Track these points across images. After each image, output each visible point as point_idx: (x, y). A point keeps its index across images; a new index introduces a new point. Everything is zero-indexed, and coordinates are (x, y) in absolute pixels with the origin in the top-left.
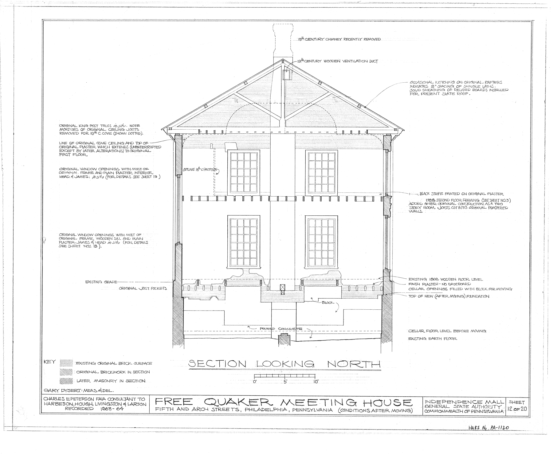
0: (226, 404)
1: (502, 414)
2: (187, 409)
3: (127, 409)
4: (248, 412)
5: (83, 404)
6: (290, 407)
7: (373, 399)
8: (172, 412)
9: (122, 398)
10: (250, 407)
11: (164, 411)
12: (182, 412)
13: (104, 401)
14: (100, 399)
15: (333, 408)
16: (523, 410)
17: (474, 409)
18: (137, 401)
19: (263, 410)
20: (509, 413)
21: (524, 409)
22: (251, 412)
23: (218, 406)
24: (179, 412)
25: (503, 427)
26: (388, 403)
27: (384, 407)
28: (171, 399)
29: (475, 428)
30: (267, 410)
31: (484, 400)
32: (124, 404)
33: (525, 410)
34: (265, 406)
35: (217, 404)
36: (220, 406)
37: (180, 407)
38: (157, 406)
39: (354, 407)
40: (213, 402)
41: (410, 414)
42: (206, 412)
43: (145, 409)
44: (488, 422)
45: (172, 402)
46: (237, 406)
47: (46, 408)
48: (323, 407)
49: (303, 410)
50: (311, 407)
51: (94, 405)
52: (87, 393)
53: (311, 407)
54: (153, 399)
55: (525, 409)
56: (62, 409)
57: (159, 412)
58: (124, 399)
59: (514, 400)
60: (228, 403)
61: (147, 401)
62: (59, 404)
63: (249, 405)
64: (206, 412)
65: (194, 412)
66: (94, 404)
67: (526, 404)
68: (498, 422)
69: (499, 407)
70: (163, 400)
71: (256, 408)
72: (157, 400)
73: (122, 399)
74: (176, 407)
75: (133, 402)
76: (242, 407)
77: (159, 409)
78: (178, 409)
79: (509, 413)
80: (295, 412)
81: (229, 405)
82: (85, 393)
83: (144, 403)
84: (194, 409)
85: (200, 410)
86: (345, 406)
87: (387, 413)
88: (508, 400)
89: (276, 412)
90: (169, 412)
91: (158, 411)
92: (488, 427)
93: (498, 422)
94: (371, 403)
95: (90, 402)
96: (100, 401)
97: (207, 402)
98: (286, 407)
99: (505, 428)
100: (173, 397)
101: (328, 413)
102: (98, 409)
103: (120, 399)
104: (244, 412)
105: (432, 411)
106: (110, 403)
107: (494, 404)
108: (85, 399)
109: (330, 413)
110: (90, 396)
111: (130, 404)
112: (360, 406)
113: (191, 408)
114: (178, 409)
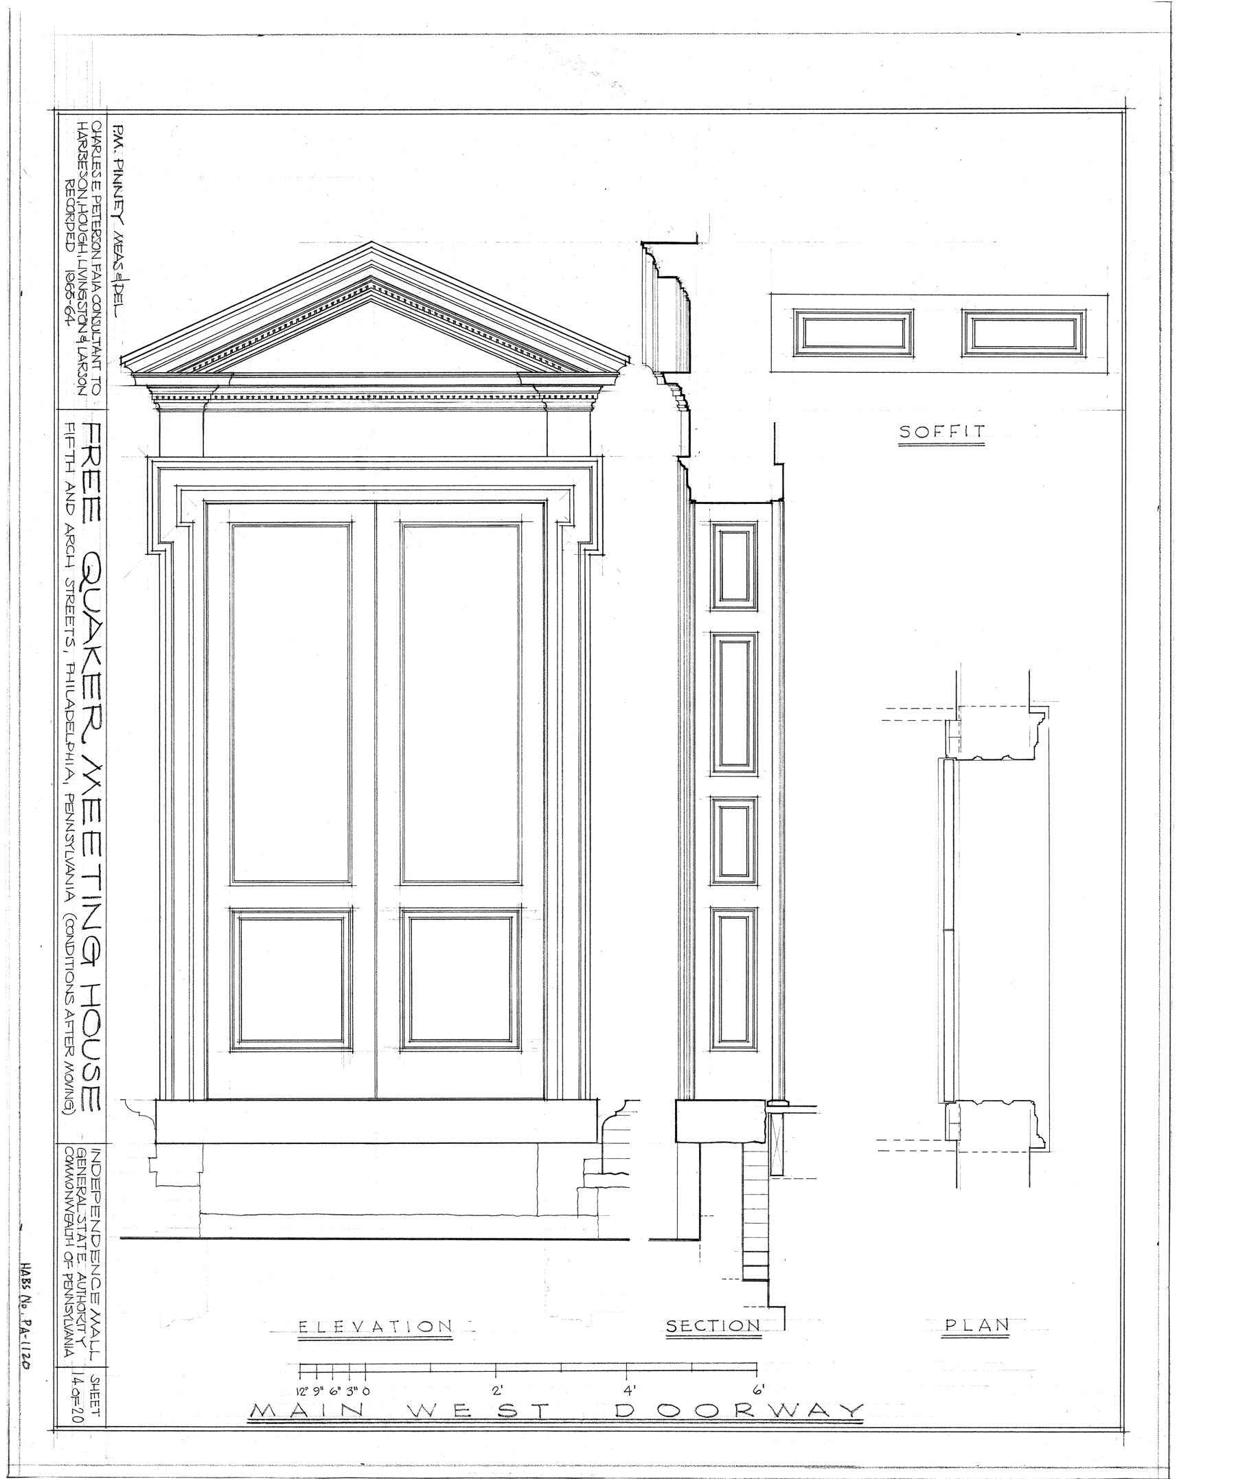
0: (84, 612)
1: (62, 1352)
2: (70, 508)
3: (70, 334)
4: (64, 669)
5: (83, 228)
6: (79, 785)
7: (101, 1009)
8: (64, 467)
9: (97, 331)
10: (77, 677)
11: (64, 443)
12: (63, 496)
13: (89, 286)
14: (97, 275)
15: (78, 901)
16: (76, 1414)
17: (76, 1278)
18: (93, 373)
19: (70, 714)
20: (65, 1377)
21: (77, 1412)
22: (64, 677)
23: (80, 591)
24: (64, 487)
25: (26, 1352)
26: (91, 1049)
27: (79, 1038)
28: (96, 463)
29: (27, 1280)
30: (70, 723)
31: (99, 1308)
32: (84, 339)
33: (75, 1419)
34: (81, 718)
35: (86, 586)
36: (79, 596)
37: (78, 489)
38: (78, 426)
39: (78, 958)
40: (92, 578)
41: (61, 1108)
42: (63, 560)
43: (69, 397)
44: (40, 1311)
45: (89, 466)
46: (79, 645)
47: (69, 125)
48: (78, 873)
49: (72, 822)
50: (78, 844)
51: (80, 258)
52: (112, 242)
53: (78, 844)
54: (99, 417)
55: (75, 1419)
56: (70, 169)
57: (60, 434)
58: (96, 336)
59: (101, 1387)
60: (91, 618)
61: (91, 401)
62: (82, 162)
63: (83, 672)
64: (63, 560)
65: (63, 529)
66: (84, 256)
67: (90, 1420)
68: (40, 1339)
69: (82, 1341)
70: (95, 444)
71: (76, 696)
72: (95, 428)
73: (95, 332)
74: (77, 479)
75: (89, 360)
76: (77, 654)
77: (72, 431)
78: (71, 487)
79: (65, 1377)
80: (64, 800)
81: (82, 622)
82: (111, 235)
83: (87, 390)
84: (70, 528)
85: (69, 544)
86: (80, 936)
87: (63, 1050)
88: (100, 1373)
89: (63, 749)
90: (63, 460)
91: (64, 429)
92: (27, 1314)
93: (40, 1339)
94: (92, 1005)
95: (88, 248)
96: (89, 275)
97: (91, 561)
98: (78, 777)
99: (27, 1359)
100: (102, 467)
101: (61, 891)
102: (69, 261)
103: (95, 328)
104: (64, 659)
105: (71, 1166)
106: (85, 300)
107: (89, 1331)
108: (95, 235)
109: (63, 896)
110: (103, 249)
111: (82, 351)
112: (85, 974)
113: (75, 521)
114: (71, 487)
